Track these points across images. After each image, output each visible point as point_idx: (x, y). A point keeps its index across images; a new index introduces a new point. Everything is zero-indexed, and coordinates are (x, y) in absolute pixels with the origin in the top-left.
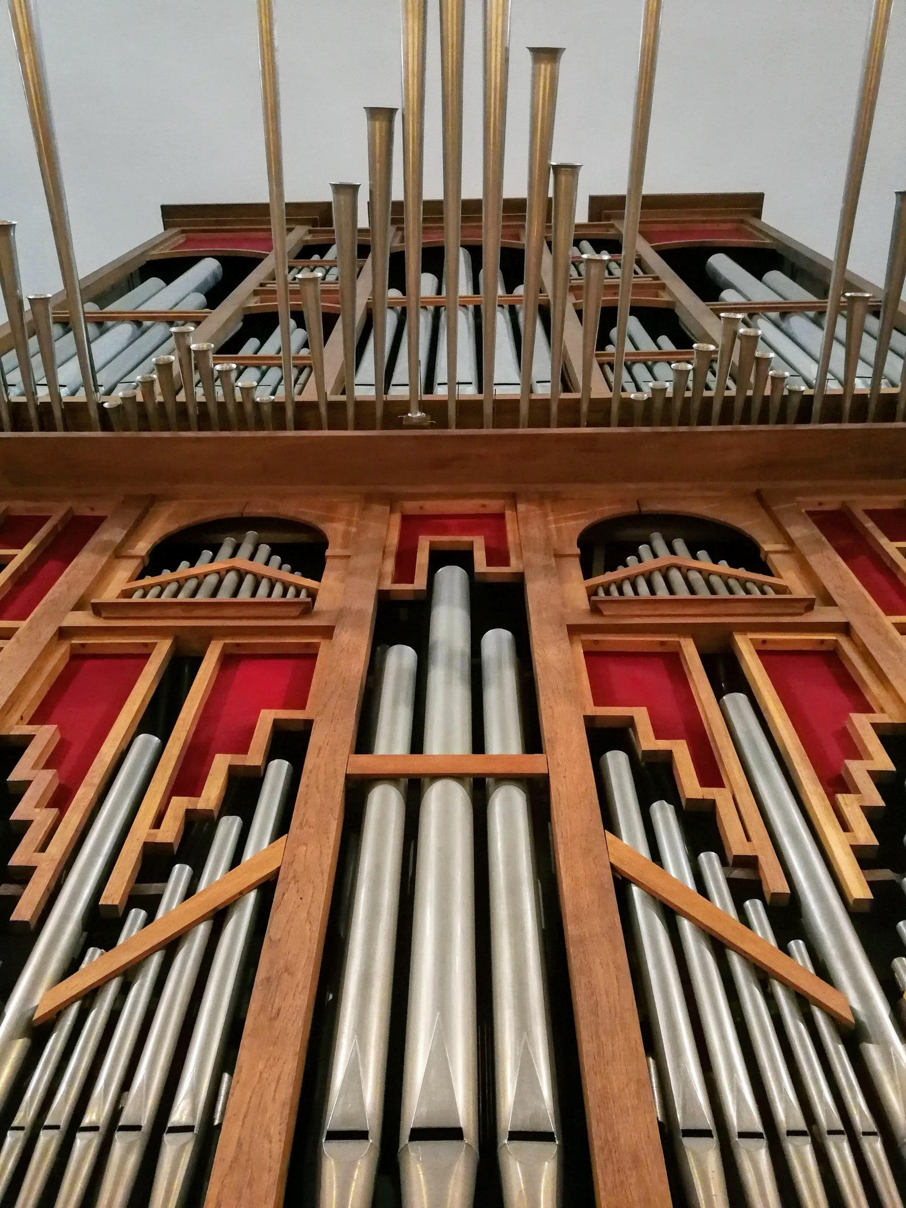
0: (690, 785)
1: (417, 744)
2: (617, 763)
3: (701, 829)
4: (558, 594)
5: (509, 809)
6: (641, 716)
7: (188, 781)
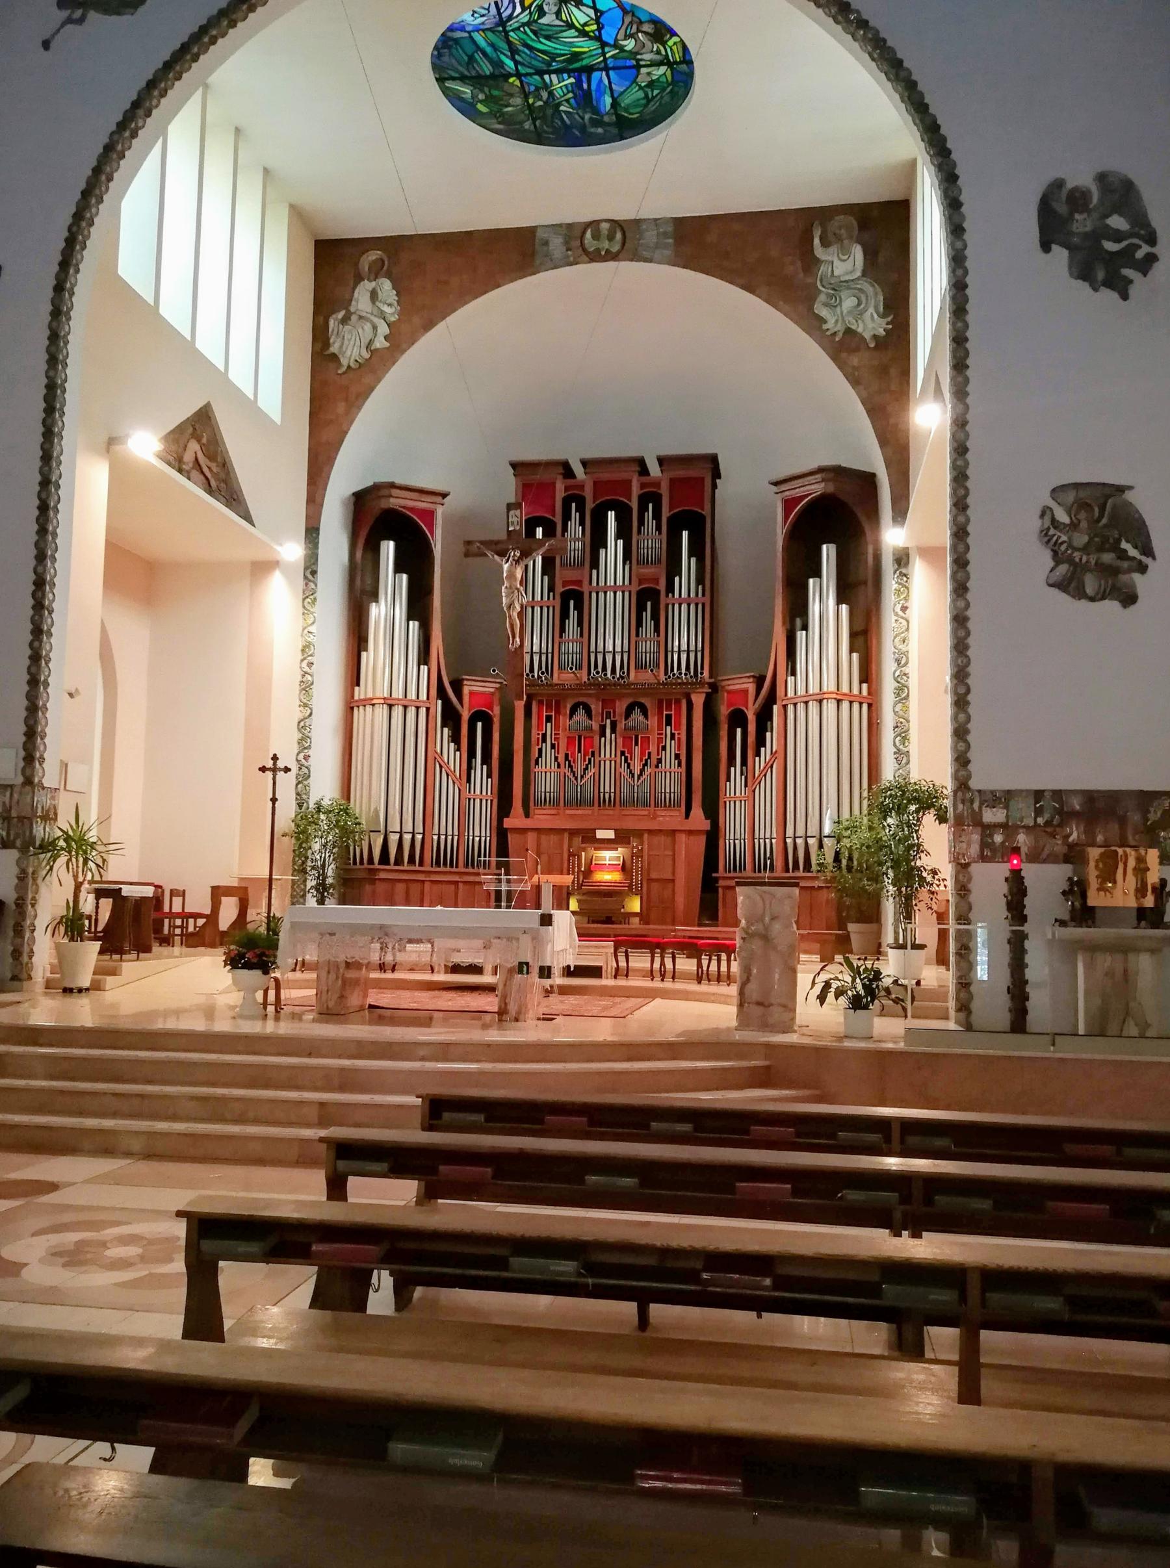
3: (629, 767)
4: (621, 726)
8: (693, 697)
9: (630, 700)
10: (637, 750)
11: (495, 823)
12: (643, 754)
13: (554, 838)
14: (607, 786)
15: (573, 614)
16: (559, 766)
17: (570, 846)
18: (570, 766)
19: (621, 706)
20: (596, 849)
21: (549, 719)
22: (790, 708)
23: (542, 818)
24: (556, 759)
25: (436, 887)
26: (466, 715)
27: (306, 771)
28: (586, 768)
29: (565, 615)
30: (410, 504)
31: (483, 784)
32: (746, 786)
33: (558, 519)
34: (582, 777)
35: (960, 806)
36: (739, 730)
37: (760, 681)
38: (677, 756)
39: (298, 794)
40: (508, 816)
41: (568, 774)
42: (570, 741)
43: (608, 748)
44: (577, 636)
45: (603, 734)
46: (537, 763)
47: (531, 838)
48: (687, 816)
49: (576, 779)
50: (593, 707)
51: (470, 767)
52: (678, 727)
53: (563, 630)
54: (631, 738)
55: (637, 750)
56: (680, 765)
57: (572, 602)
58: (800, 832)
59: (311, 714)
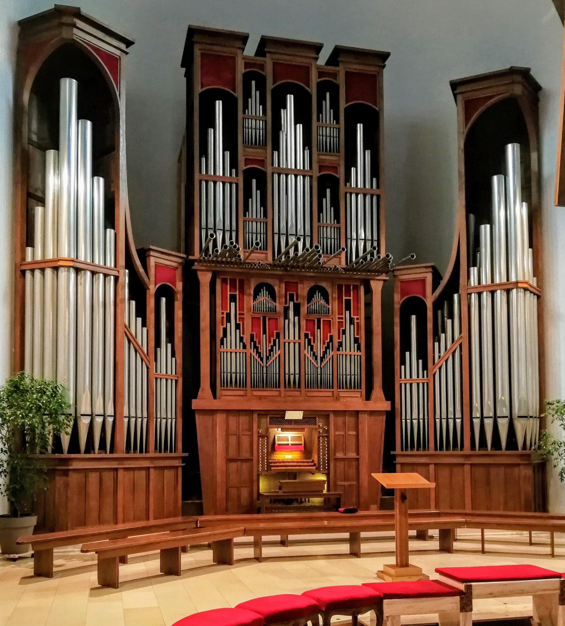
0: (312, 344)
1: (289, 338)
2: (307, 340)
4: (304, 310)
5: (297, 345)
6: (309, 333)
7: (270, 342)
8: (373, 284)
9: (312, 284)
11: (180, 404)
12: (325, 337)
13: (244, 419)
14: (292, 368)
15: (256, 194)
16: (244, 347)
17: (259, 427)
18: (256, 347)
19: (304, 289)
20: (283, 430)
21: (233, 298)
23: (230, 399)
28: (271, 350)
29: (248, 195)
31: (168, 363)
32: (425, 367)
38: (356, 340)
40: (196, 398)
41: (254, 354)
43: (292, 330)
44: (260, 216)
45: (286, 317)
46: (222, 343)
47: (220, 418)
48: (368, 397)
49: (262, 360)
50: (276, 289)
53: (246, 209)
54: (315, 322)
55: (319, 333)
56: (359, 348)
57: (254, 181)
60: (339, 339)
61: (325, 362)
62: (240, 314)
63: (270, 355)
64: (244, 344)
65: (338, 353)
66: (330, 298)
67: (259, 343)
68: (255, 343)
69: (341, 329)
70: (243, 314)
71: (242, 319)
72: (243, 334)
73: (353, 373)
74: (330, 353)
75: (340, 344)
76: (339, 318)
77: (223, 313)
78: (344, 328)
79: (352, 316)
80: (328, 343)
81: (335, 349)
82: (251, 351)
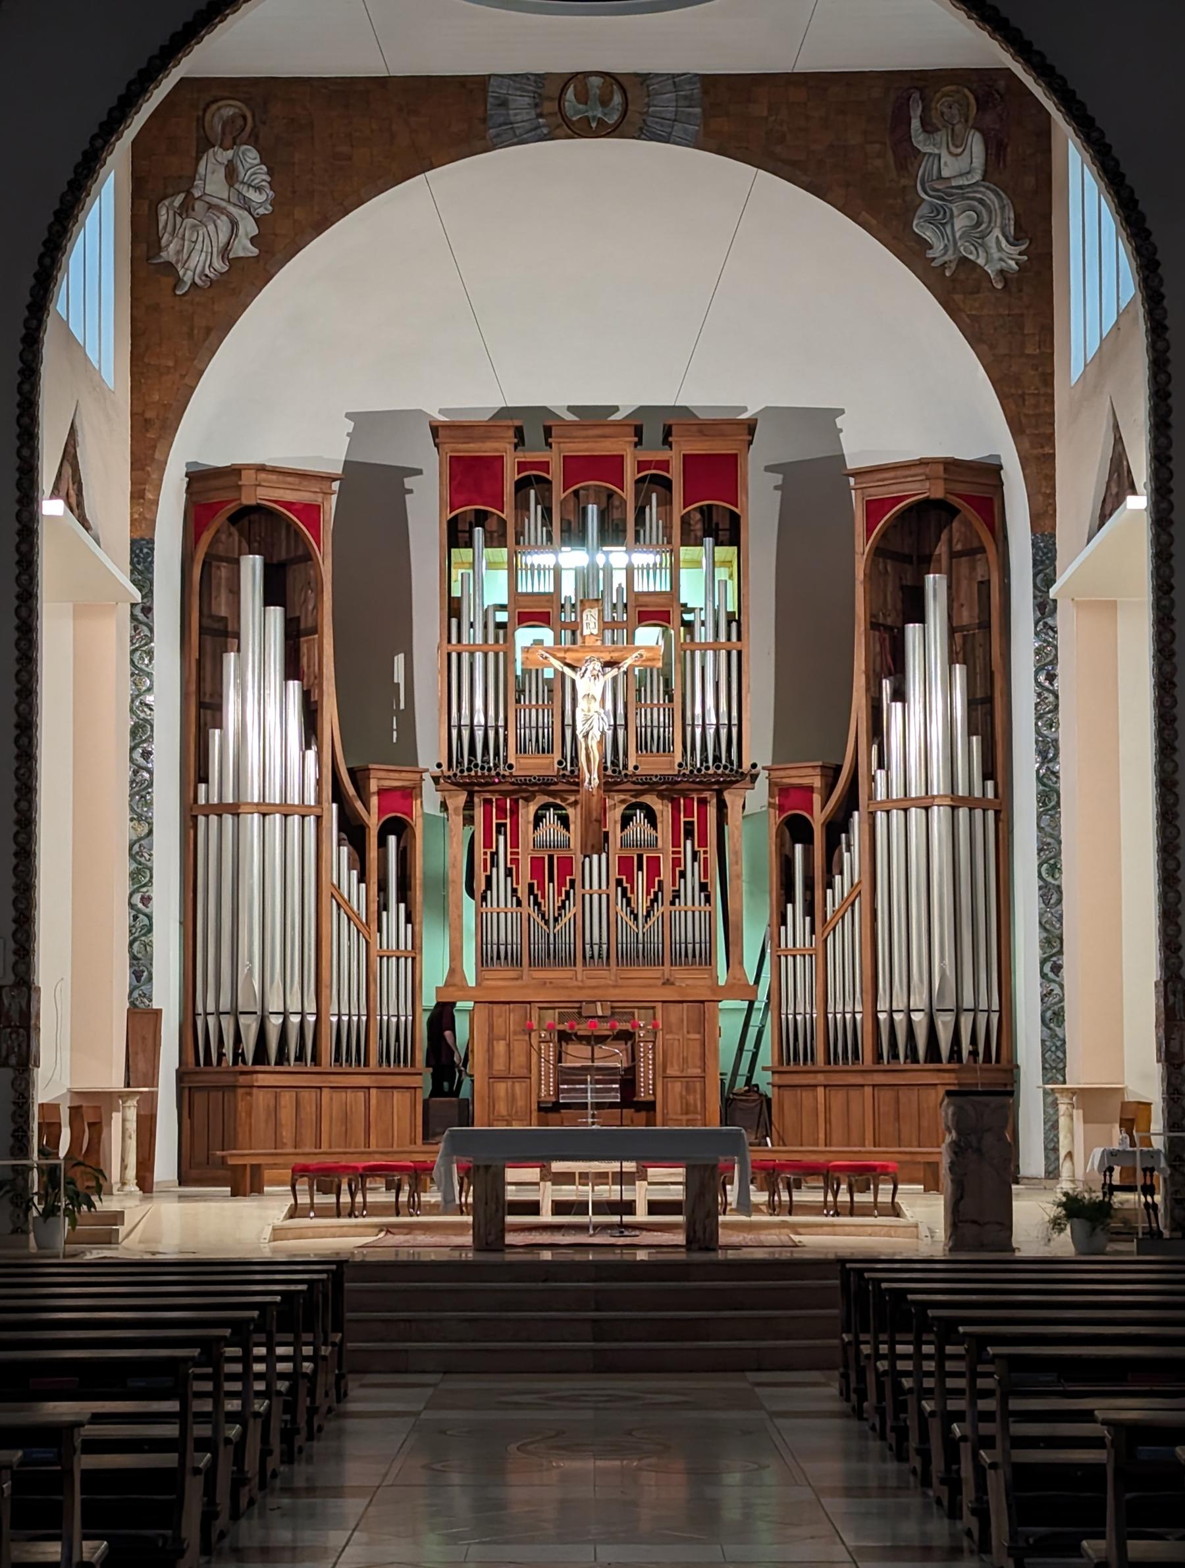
0: (629, 895)
3: (629, 904)
5: (604, 897)
7: (560, 894)
8: (727, 796)
10: (641, 878)
12: (650, 884)
16: (519, 903)
18: (537, 903)
22: (880, 817)
24: (514, 891)
25: (340, 1096)
26: (373, 822)
27: (146, 922)
28: (563, 906)
30: (290, 496)
32: (813, 932)
33: (508, 514)
34: (556, 920)
35: (1171, 999)
36: (799, 848)
37: (831, 773)
38: (703, 887)
39: (134, 958)
41: (534, 915)
42: (536, 863)
51: (384, 906)
52: (703, 842)
55: (641, 878)
58: (899, 1003)
59: (150, 832)
60: (674, 885)
61: (650, 923)
62: (512, 853)
63: (560, 915)
64: (518, 899)
65: (673, 908)
66: (659, 820)
67: (543, 897)
68: (536, 897)
69: (677, 870)
70: (518, 853)
71: (515, 861)
72: (518, 883)
73: (697, 940)
74: (659, 910)
75: (676, 895)
76: (673, 852)
77: (485, 853)
78: (682, 868)
79: (696, 848)
80: (656, 894)
81: (667, 903)
82: (528, 909)
